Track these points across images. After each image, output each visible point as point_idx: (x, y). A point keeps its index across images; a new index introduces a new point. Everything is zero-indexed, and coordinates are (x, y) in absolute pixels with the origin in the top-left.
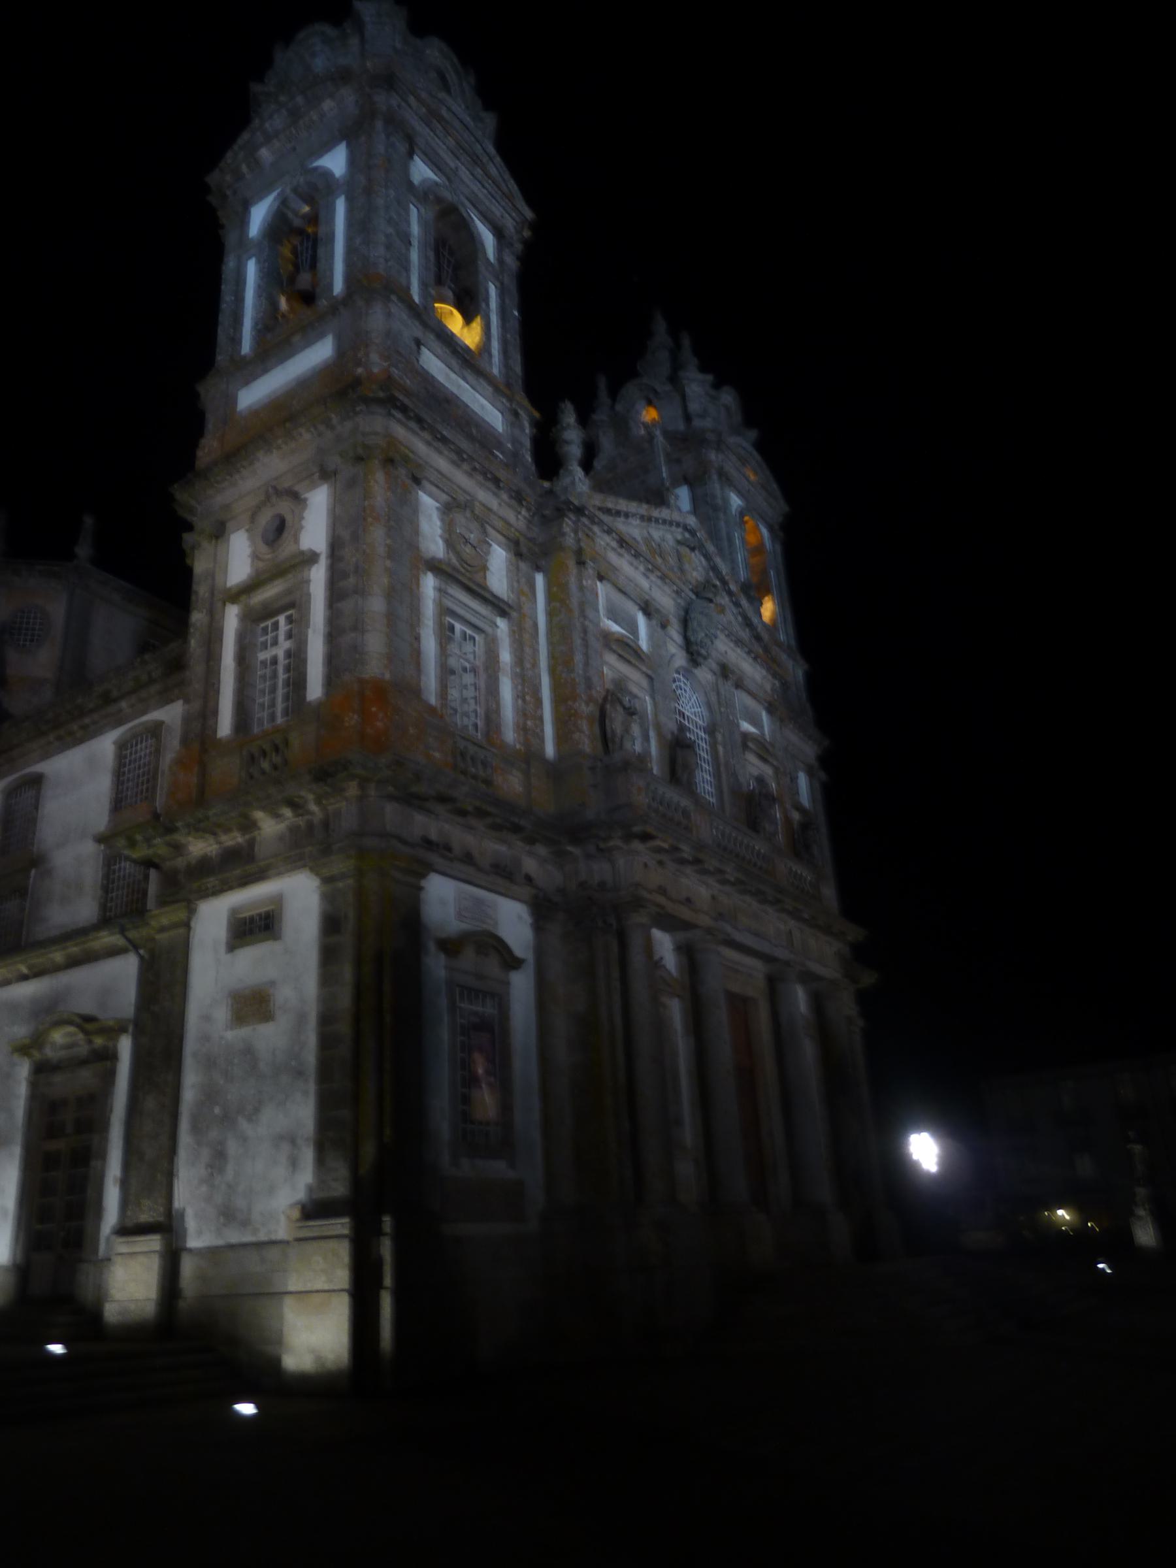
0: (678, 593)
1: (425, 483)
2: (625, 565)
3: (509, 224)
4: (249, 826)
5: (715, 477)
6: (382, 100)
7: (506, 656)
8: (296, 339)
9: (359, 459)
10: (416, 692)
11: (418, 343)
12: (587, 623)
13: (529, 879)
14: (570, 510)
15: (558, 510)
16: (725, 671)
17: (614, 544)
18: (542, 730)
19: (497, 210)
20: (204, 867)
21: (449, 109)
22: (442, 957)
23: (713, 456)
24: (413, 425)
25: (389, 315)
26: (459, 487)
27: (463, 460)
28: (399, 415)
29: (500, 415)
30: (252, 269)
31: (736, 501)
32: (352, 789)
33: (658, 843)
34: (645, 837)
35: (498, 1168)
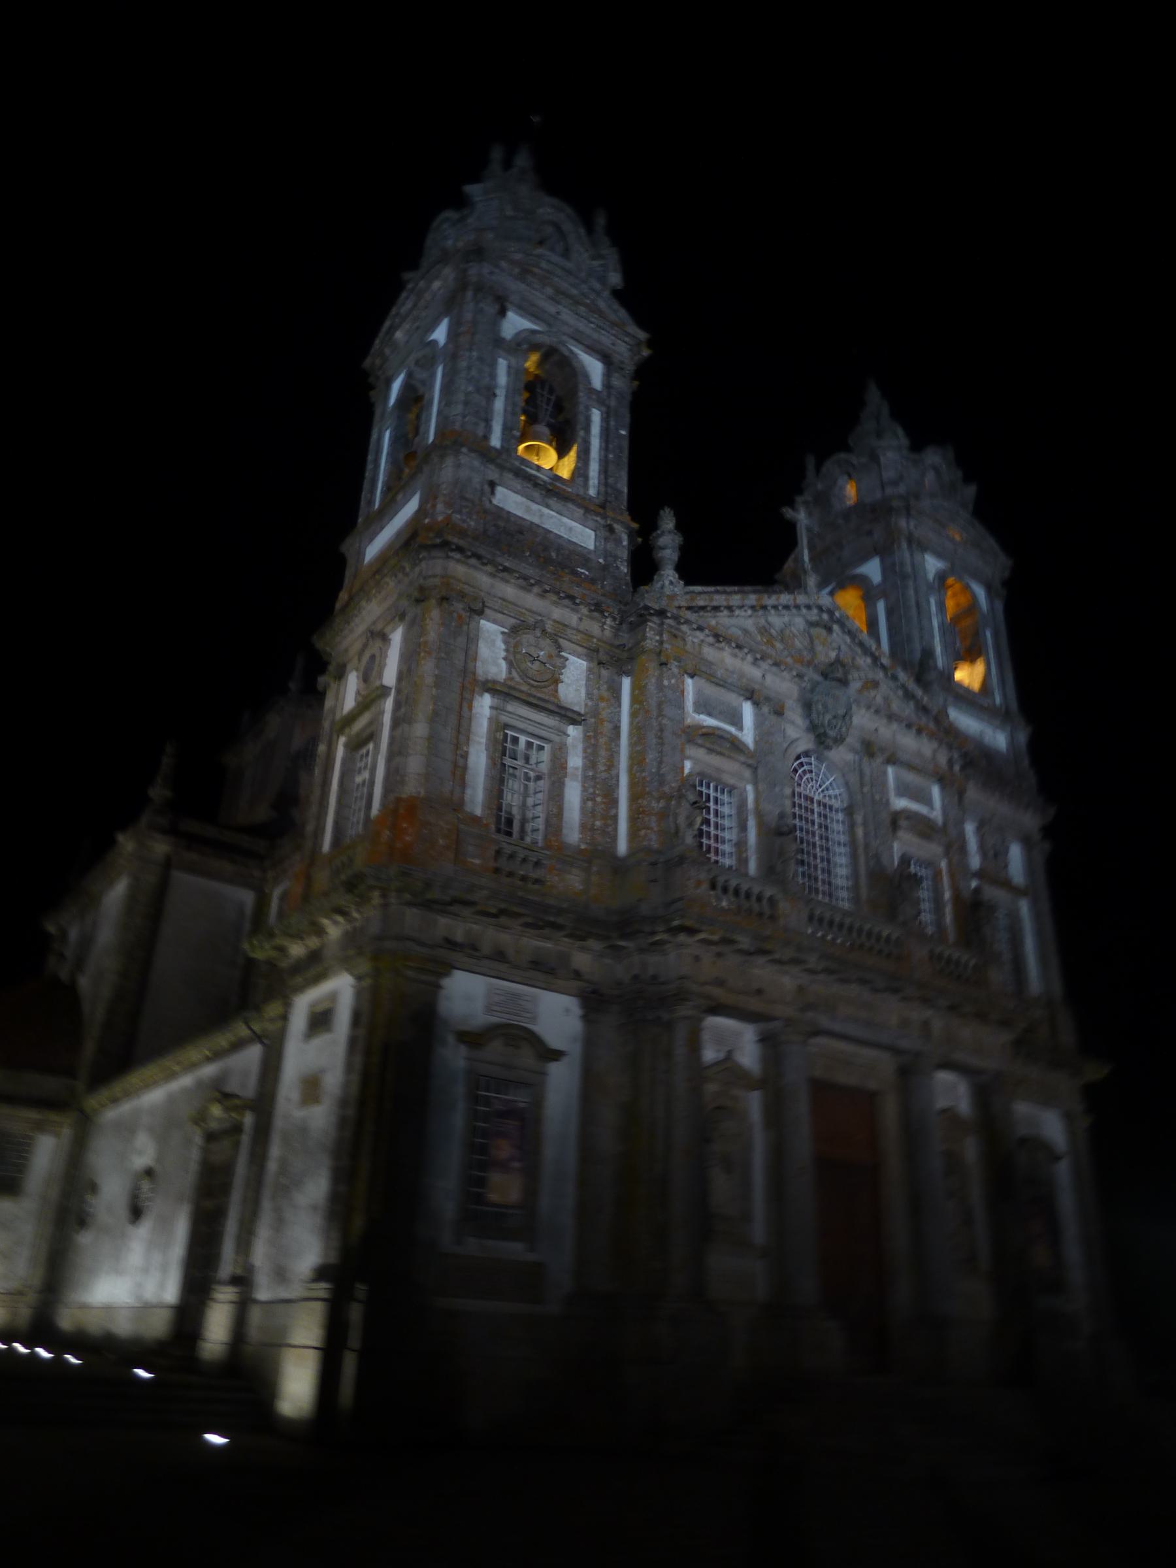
0: (800, 676)
1: (487, 611)
2: (726, 659)
3: (622, 350)
4: (320, 932)
5: (904, 545)
6: (473, 271)
7: (575, 761)
8: (399, 497)
9: (418, 601)
10: (457, 806)
11: (492, 485)
12: (665, 721)
13: (577, 975)
14: (651, 614)
15: (641, 615)
16: (869, 748)
17: (711, 640)
18: (616, 830)
19: (606, 339)
20: (299, 967)
21: (549, 261)
22: (463, 1050)
23: (903, 523)
24: (473, 561)
25: (458, 466)
26: (526, 609)
27: (532, 585)
28: (458, 556)
29: (592, 533)
30: (387, 435)
31: (932, 565)
32: (376, 898)
33: (702, 936)
34: (691, 931)
35: (515, 1250)
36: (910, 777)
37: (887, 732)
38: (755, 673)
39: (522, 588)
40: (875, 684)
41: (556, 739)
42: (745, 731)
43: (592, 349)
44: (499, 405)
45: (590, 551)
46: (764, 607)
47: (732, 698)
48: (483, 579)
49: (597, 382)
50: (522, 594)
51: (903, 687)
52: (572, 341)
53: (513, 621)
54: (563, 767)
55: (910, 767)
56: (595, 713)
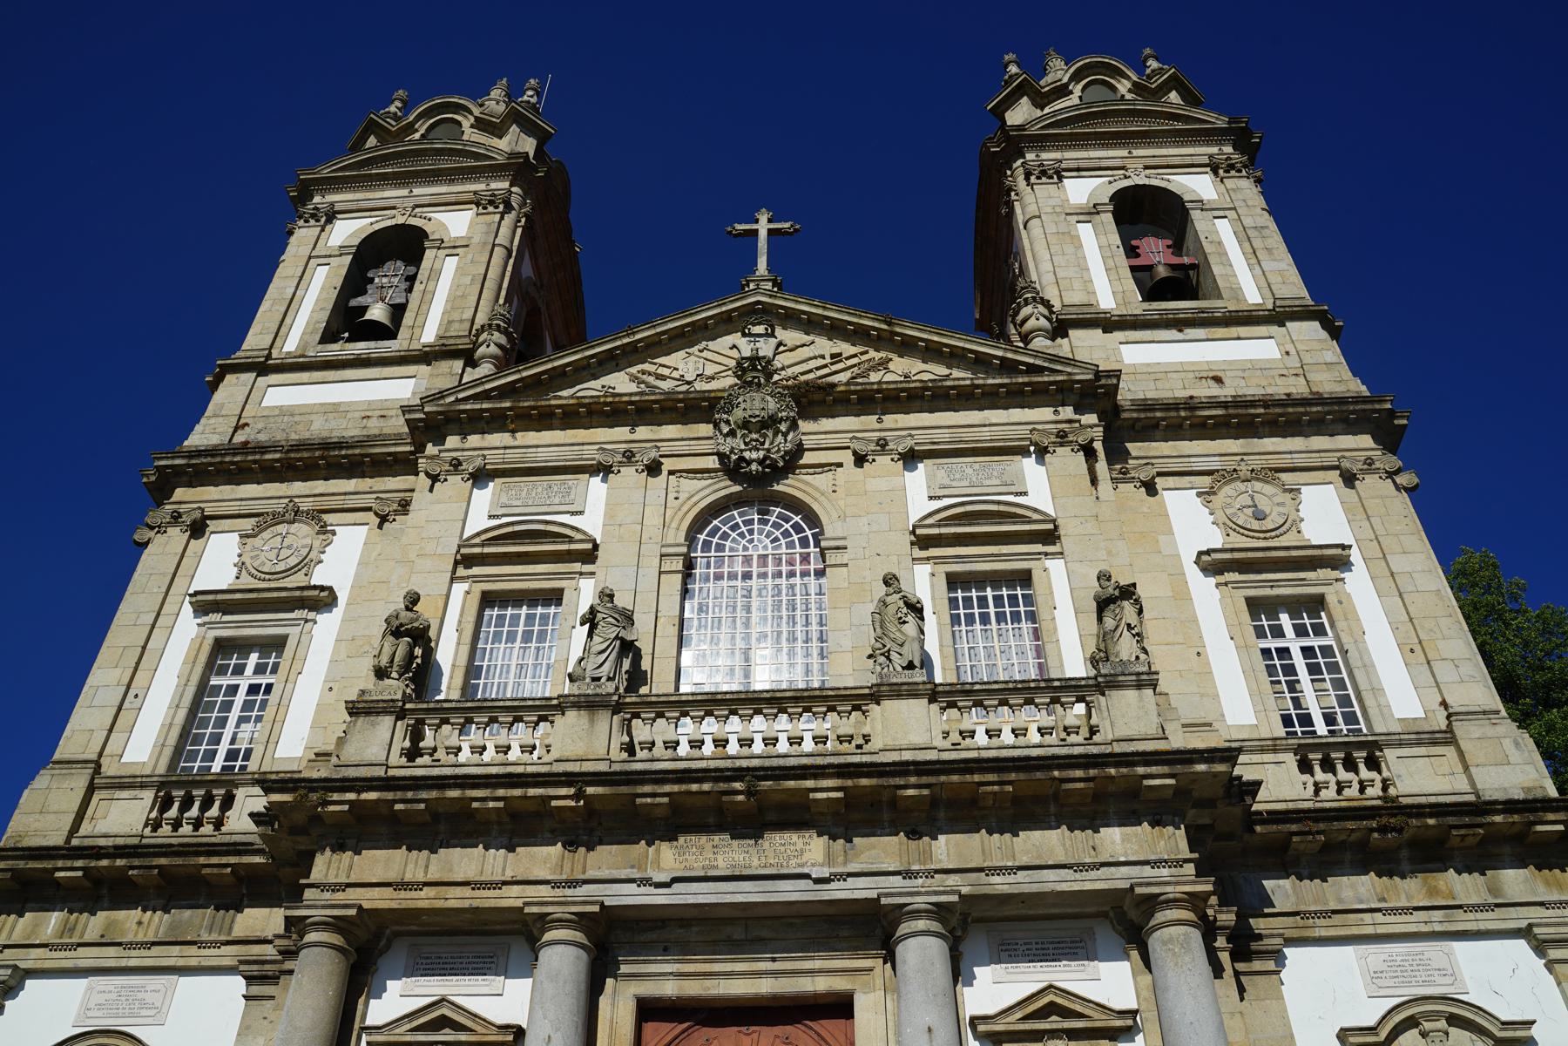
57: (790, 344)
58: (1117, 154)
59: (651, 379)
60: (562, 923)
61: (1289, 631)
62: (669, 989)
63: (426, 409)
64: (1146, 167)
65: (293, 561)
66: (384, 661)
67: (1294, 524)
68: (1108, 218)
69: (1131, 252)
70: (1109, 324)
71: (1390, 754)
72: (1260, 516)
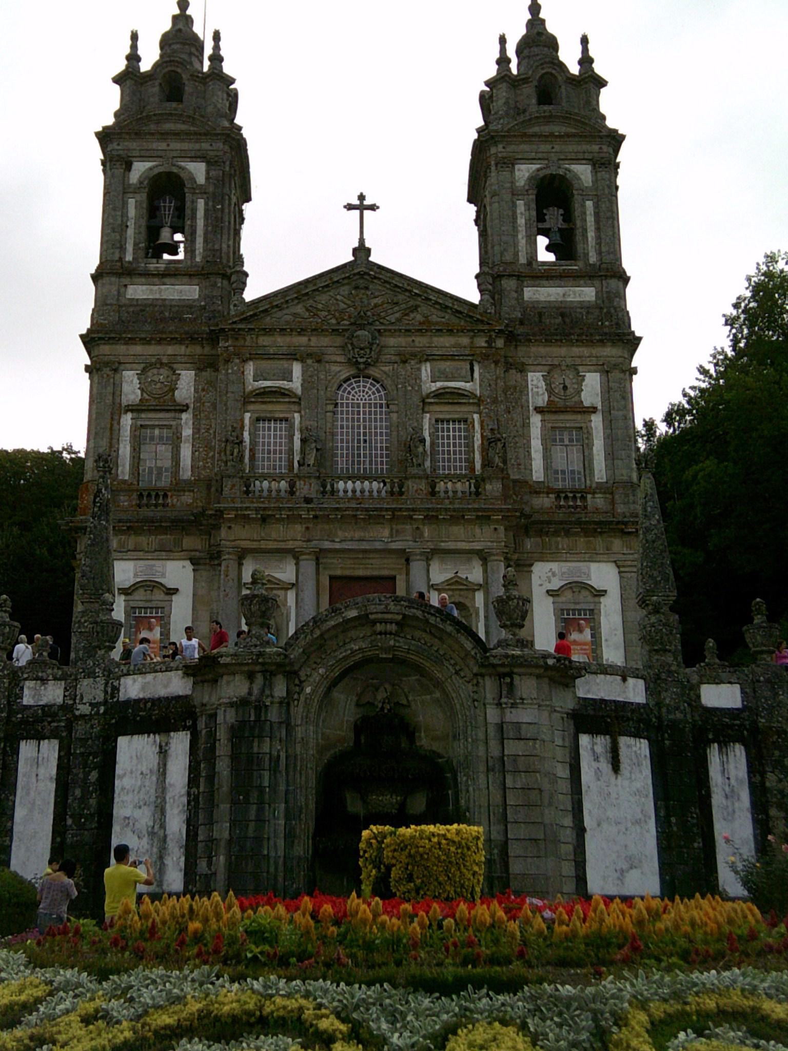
7: (187, 432)
11: (126, 286)
17: (263, 332)
36: (446, 365)
37: (421, 341)
38: (303, 340)
39: (143, 344)
40: (415, 308)
41: (173, 423)
42: (294, 379)
43: (195, 158)
44: (130, 232)
45: (194, 300)
46: (307, 294)
47: (285, 364)
48: (121, 349)
49: (201, 179)
50: (147, 347)
51: (437, 303)
52: (179, 159)
53: (142, 365)
54: (178, 437)
55: (445, 358)
56: (198, 400)
57: (376, 294)
58: (545, 147)
59: (314, 311)
60: (305, 554)
61: (567, 442)
62: (339, 573)
63: (220, 326)
64: (559, 159)
65: (166, 389)
66: (228, 452)
67: (579, 391)
68: (534, 197)
69: (541, 218)
70: (519, 277)
71: (589, 496)
72: (565, 388)
